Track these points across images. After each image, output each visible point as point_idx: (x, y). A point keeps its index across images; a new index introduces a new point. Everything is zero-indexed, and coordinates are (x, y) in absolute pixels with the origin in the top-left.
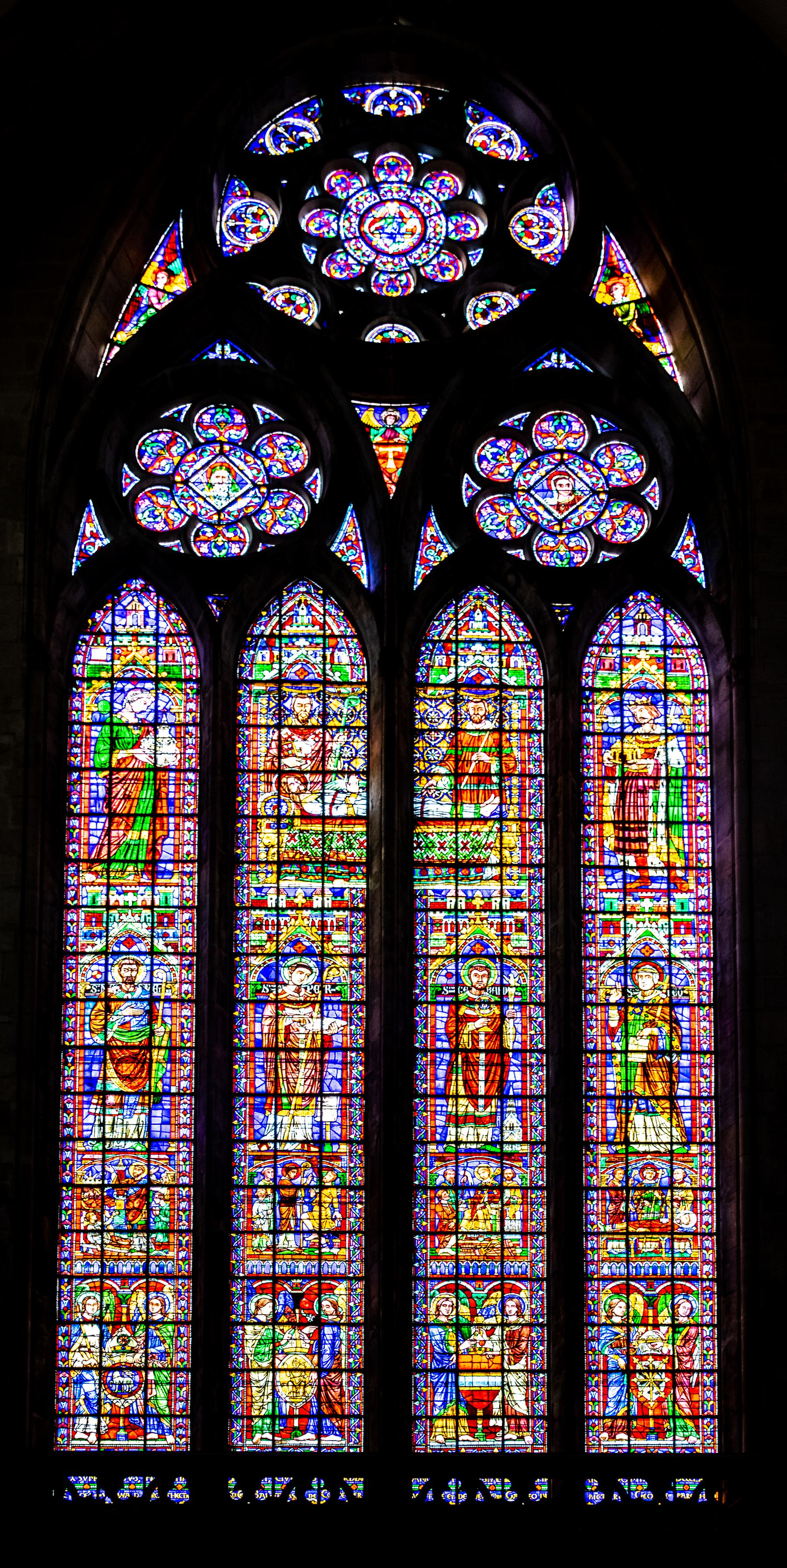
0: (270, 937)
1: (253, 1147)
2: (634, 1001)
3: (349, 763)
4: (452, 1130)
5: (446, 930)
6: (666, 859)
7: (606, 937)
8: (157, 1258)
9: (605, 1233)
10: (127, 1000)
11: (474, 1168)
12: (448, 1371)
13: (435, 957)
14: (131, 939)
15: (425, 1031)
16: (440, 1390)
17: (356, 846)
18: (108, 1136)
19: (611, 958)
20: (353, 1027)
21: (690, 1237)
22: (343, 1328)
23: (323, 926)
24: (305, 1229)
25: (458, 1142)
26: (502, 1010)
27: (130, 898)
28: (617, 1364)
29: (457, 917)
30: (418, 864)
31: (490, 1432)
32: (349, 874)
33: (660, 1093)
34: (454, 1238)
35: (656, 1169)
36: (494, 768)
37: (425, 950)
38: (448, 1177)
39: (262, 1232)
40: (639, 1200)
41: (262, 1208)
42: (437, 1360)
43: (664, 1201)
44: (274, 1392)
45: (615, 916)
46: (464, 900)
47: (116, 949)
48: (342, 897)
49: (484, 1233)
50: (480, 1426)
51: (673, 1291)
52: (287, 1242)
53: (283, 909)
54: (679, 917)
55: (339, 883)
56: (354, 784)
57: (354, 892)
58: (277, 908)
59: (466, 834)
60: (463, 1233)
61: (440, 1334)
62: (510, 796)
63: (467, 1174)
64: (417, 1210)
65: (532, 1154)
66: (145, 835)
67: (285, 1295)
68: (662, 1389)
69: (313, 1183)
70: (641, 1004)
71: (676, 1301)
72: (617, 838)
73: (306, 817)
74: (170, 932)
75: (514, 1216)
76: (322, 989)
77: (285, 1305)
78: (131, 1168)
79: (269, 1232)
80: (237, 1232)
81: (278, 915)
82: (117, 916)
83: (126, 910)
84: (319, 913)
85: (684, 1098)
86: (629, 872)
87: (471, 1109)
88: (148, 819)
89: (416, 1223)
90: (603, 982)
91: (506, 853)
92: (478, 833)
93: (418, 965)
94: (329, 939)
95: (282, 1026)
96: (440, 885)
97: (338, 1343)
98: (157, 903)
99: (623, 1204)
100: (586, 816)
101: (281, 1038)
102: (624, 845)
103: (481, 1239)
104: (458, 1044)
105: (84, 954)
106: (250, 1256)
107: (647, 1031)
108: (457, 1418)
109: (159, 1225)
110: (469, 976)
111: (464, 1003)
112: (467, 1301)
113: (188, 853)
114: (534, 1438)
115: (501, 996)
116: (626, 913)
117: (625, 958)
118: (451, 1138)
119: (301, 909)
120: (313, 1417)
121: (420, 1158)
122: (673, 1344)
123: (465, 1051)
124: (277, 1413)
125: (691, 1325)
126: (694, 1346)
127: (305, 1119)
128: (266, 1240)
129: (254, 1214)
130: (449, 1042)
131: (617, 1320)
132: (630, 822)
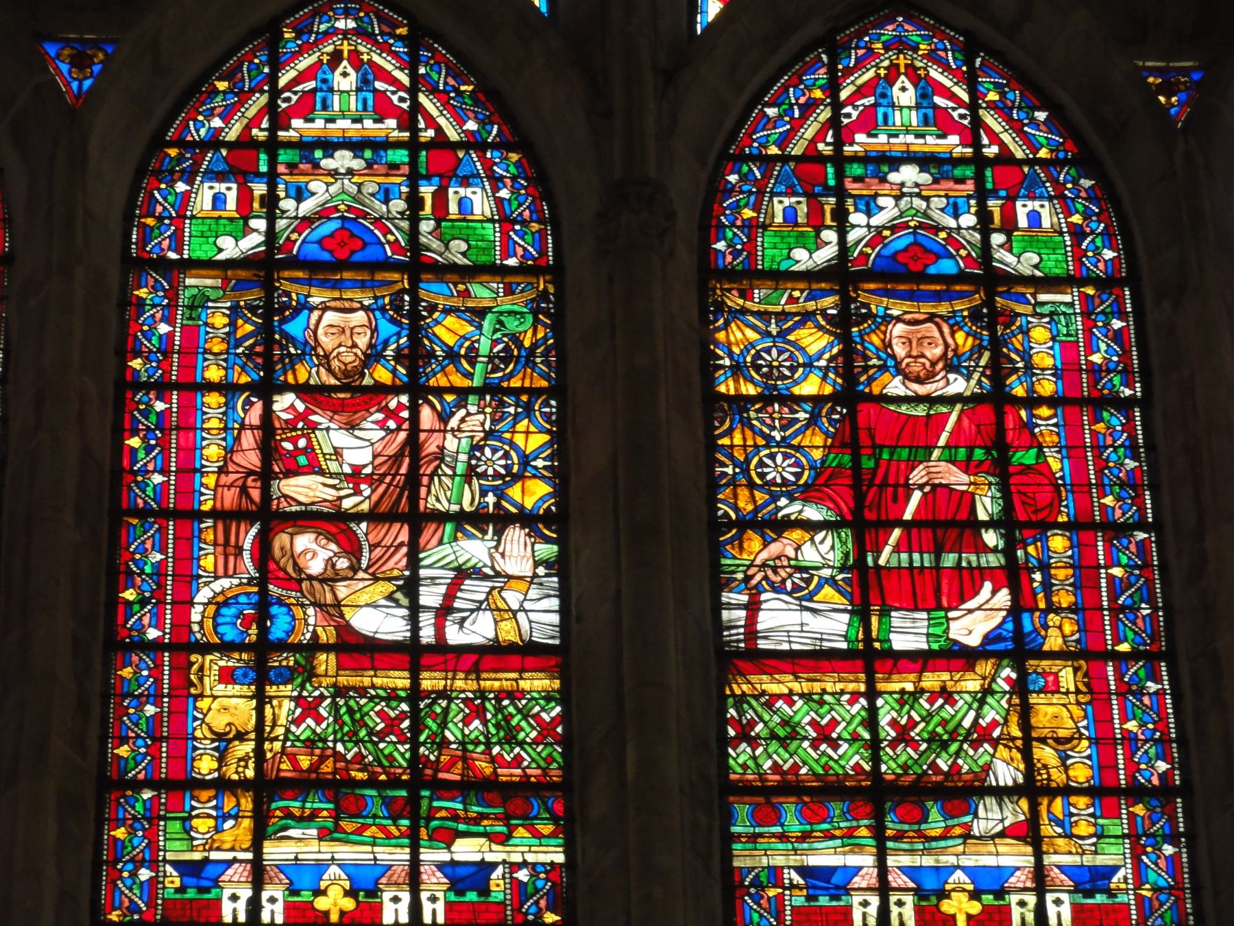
3: (501, 494)
30: (745, 790)
32: (505, 819)
46: (909, 899)
48: (485, 891)
55: (467, 850)
57: (523, 875)
62: (1047, 585)
91: (1046, 754)
92: (947, 695)
96: (824, 857)
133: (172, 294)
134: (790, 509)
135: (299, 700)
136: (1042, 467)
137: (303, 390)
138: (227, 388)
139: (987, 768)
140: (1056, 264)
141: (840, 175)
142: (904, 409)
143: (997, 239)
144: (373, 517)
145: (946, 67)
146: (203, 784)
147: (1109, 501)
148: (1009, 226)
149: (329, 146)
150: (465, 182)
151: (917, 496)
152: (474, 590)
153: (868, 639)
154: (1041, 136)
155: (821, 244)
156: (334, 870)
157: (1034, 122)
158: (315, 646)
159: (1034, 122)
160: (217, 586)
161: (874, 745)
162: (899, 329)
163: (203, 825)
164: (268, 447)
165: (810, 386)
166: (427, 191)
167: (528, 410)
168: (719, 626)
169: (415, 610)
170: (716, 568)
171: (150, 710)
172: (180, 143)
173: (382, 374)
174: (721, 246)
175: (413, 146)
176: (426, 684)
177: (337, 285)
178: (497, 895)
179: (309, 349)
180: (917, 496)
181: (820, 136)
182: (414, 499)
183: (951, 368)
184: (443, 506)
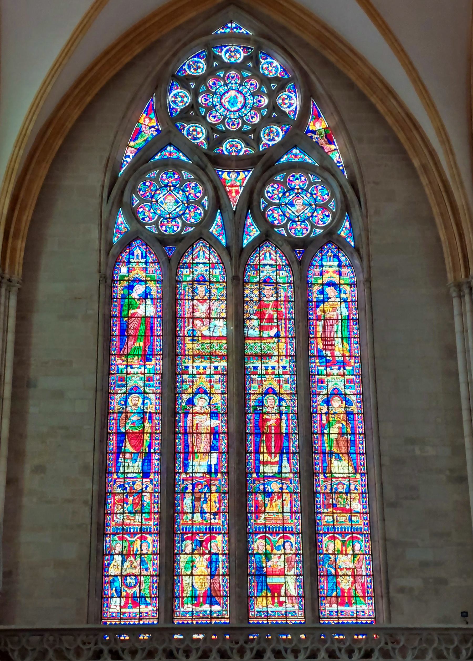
0: (190, 386)
1: (183, 476)
2: (332, 412)
4: (262, 468)
8: (145, 524)
9: (324, 513)
12: (263, 575)
13: (254, 394)
14: (137, 388)
15: (250, 425)
16: (260, 584)
17: (223, 348)
18: (126, 471)
20: (222, 424)
21: (358, 515)
25: (264, 473)
29: (262, 378)
33: (343, 451)
34: (264, 514)
35: (343, 484)
36: (275, 316)
41: (188, 502)
44: (193, 586)
45: (323, 376)
52: (197, 517)
54: (348, 376)
55: (216, 364)
59: (265, 344)
70: (335, 413)
72: (323, 344)
73: (204, 337)
76: (210, 408)
78: (135, 485)
79: (190, 513)
80: (177, 513)
81: (193, 377)
84: (209, 376)
85: (353, 453)
95: (195, 424)
96: (255, 365)
97: (218, 562)
98: (146, 372)
99: (331, 500)
101: (195, 428)
106: (182, 524)
107: (338, 425)
108: (267, 597)
110: (267, 402)
111: (265, 413)
115: (280, 411)
116: (327, 375)
117: (327, 394)
123: (266, 433)
131: (330, 552)
132: (327, 338)
134: (253, 317)
138: (188, 300)
144: (205, 318)
146: (187, 355)
158: (199, 336)
161: (261, 350)
163: (187, 361)
164: (193, 308)
168: (244, 333)
171: (181, 345)
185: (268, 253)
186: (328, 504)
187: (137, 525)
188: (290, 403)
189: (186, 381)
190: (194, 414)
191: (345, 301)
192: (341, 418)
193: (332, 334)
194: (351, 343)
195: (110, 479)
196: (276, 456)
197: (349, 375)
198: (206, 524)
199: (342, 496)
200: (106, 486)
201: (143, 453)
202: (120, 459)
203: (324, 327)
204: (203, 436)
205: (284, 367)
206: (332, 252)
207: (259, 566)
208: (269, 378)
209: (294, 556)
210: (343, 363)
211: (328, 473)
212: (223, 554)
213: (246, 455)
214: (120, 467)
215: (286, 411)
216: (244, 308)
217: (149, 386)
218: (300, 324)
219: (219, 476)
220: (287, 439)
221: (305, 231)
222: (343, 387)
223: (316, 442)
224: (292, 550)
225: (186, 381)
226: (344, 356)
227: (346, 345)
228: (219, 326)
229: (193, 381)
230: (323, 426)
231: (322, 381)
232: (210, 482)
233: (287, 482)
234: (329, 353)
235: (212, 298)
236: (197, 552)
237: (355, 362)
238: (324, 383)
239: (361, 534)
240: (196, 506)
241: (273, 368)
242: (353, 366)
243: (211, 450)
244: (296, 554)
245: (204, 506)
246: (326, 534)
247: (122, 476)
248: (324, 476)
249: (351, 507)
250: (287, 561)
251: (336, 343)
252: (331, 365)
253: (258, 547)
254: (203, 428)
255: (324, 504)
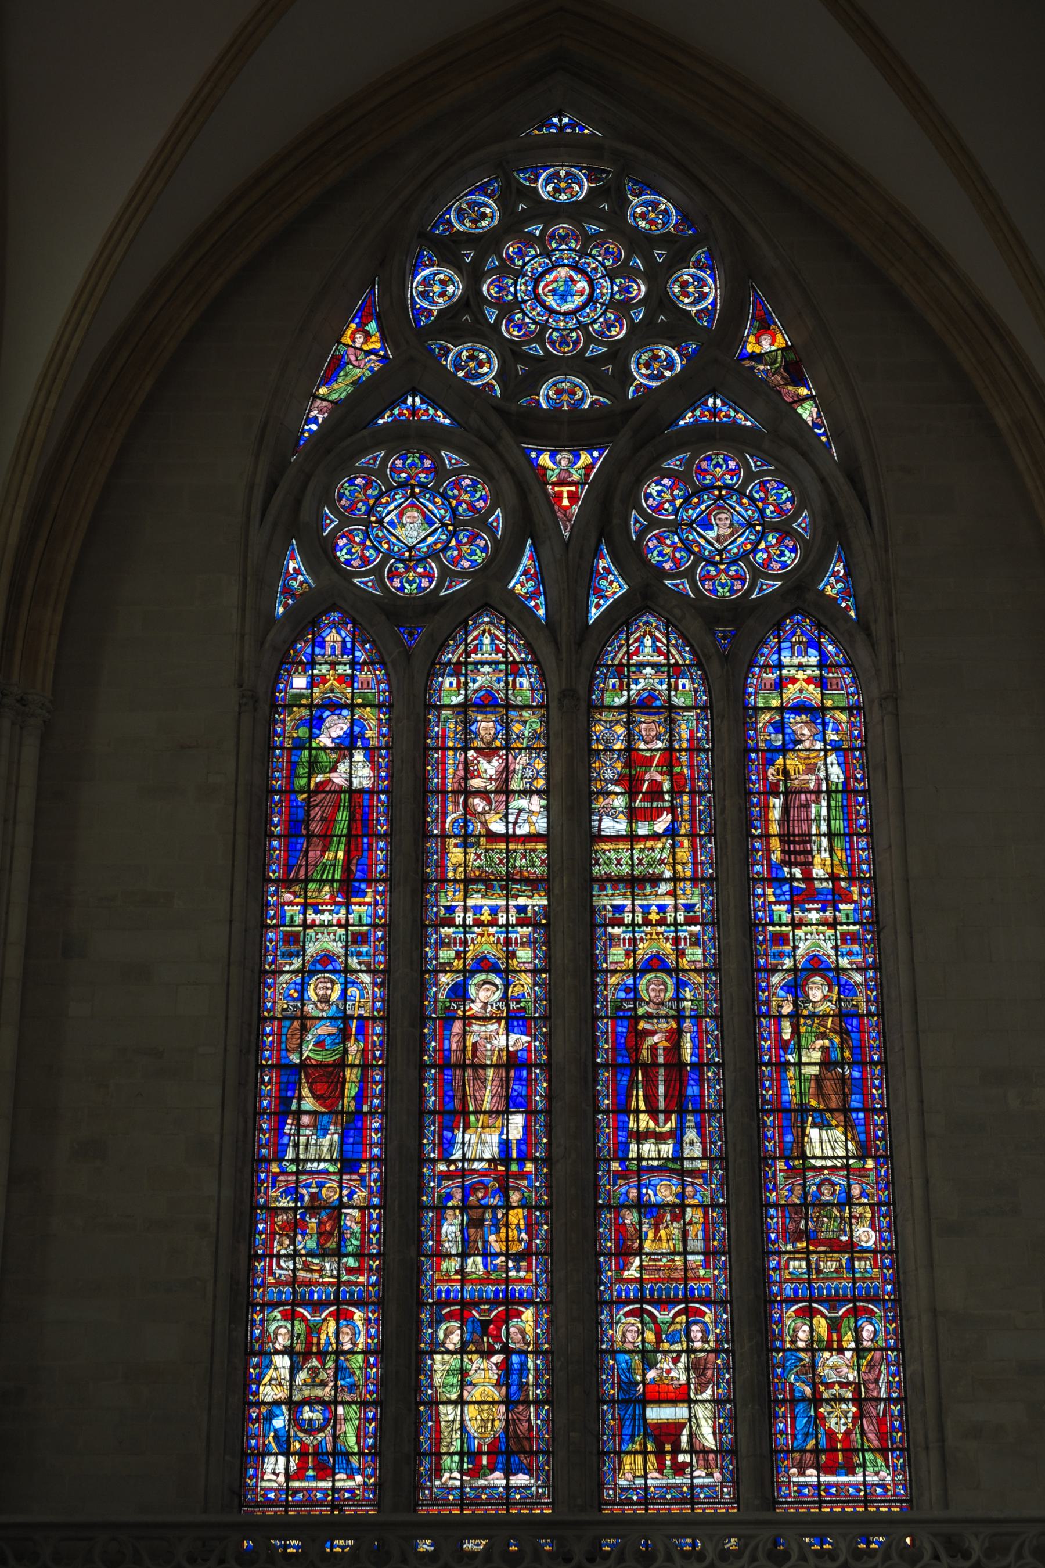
0: (458, 953)
1: (442, 1167)
2: (805, 1012)
3: (531, 784)
4: (634, 1147)
5: (624, 945)
6: (829, 870)
7: (776, 949)
8: (349, 1283)
9: (786, 1252)
10: (322, 1018)
11: (655, 1186)
12: (637, 1401)
13: (615, 971)
14: (327, 958)
15: (606, 1047)
16: (627, 1423)
17: (538, 863)
18: (301, 1156)
19: (782, 970)
20: (537, 1043)
21: (869, 1255)
22: (531, 1356)
23: (508, 942)
24: (493, 1251)
25: (640, 1158)
26: (679, 1024)
27: (326, 917)
28: (803, 1393)
29: (634, 932)
30: (597, 880)
31: (679, 1469)
32: (531, 891)
33: (833, 1105)
34: (638, 1259)
35: (833, 1184)
36: (666, 787)
37: (605, 965)
38: (631, 1195)
39: (449, 1256)
40: (818, 1218)
41: (450, 1229)
42: (624, 1390)
43: (842, 1218)
44: (463, 1428)
45: (784, 928)
46: (640, 915)
47: (313, 968)
49: (667, 1254)
50: (668, 1463)
51: (855, 1312)
52: (475, 1265)
53: (470, 926)
54: (845, 927)
55: (522, 901)
56: (536, 803)
57: (536, 908)
58: (464, 925)
59: (641, 851)
60: (647, 1254)
61: (626, 1362)
62: (682, 812)
63: (650, 1192)
64: (601, 1230)
65: (711, 1170)
66: (341, 855)
67: (473, 1321)
68: (850, 1420)
69: (500, 1203)
70: (813, 1015)
71: (859, 1323)
72: (783, 851)
73: (492, 837)
74: (364, 949)
75: (696, 1235)
76: (508, 1006)
77: (473, 1332)
78: (324, 1191)
79: (457, 1255)
80: (426, 1256)
81: (465, 933)
82: (313, 934)
83: (322, 929)
84: (503, 929)
85: (857, 1110)
86: (795, 884)
87: (652, 1125)
88: (344, 839)
89: (600, 1244)
90: (775, 994)
91: (679, 868)
92: (653, 849)
93: (598, 980)
94: (512, 955)
96: (618, 902)
98: (351, 921)
99: (803, 1222)
100: (753, 831)
101: (469, 1054)
102: (790, 858)
103: (665, 1260)
104: (637, 1059)
105: (283, 972)
106: (439, 1281)
107: (819, 1043)
108: (644, 1453)
109: (350, 1249)
110: (647, 990)
111: (642, 1017)
112: (652, 1326)
113: (381, 873)
114: (723, 1475)
115: (678, 1010)
116: (796, 924)
117: (794, 970)
118: (633, 1154)
119: (488, 925)
120: (502, 1453)
121: (603, 1176)
122: (859, 1370)
123: (645, 1066)
124: (466, 1450)
125: (875, 1350)
126: (880, 1372)
127: (493, 1138)
128: (454, 1264)
129: (443, 1236)
130: (629, 1057)
131: (801, 1344)
132: (794, 835)
133: (439, 717)
134: (612, 788)
135: (476, 854)
136: (682, 773)
137: (476, 749)
138: (455, 749)
139: (663, 872)
140: (689, 702)
141: (629, 671)
142: (644, 753)
143: (673, 693)
144: (496, 792)
145: (661, 632)
146: (450, 881)
147: (700, 783)
148: (676, 689)
149: (483, 663)
150: (521, 676)
151: (647, 783)
152: (524, 816)
153: (632, 831)
154: (687, 656)
155: (622, 696)
156: (485, 908)
157: (685, 651)
158: (480, 835)
159: (685, 651)
160: (454, 815)
161: (632, 866)
162: (644, 725)
163: (450, 894)
164: (466, 769)
165: (618, 746)
166: (510, 679)
167: (539, 756)
168: (591, 827)
169: (507, 823)
170: (590, 808)
171: (435, 857)
172: (440, 663)
173: (498, 743)
174: (594, 697)
175: (506, 663)
176: (510, 847)
177: (485, 713)
178: (530, 914)
179: (477, 734)
180: (647, 783)
181: (623, 657)
182: (507, 786)
183: (659, 739)
184: (515, 788)
185: (648, 637)
186: (794, 1232)
187: (329, 1283)
188: (703, 992)
189: (449, 944)
190: (468, 1020)
191: (836, 748)
192: (829, 1026)
193: (805, 827)
194: (852, 849)
195: (263, 1175)
196: (667, 1120)
197: (848, 924)
198: (497, 1282)
199: (831, 1211)
200: (254, 1189)
201: (342, 1112)
202: (288, 1127)
203: (786, 810)
204: (490, 1072)
205: (689, 907)
206: (803, 633)
207: (626, 1380)
208: (651, 934)
209: (712, 1356)
210: (833, 895)
211: (798, 1158)
212: (537, 1353)
213: (594, 1117)
214: (287, 1145)
215: (692, 1010)
216: (590, 767)
217: (359, 954)
218: (727, 802)
219: (529, 1167)
220: (695, 1077)
221: (738, 586)
222: (832, 952)
223: (767, 1084)
224: (708, 1342)
225: (449, 944)
226: (834, 878)
227: (839, 853)
228: (531, 812)
229: (464, 943)
230: (783, 1046)
231: (781, 939)
232: (508, 1182)
233: (696, 1181)
234: (797, 872)
235: (514, 745)
236: (474, 1349)
237: (861, 893)
238: (788, 945)
239: (876, 1300)
240: (472, 1238)
241: (662, 908)
242: (855, 902)
243: (508, 1106)
244: (716, 1351)
245: (492, 1238)
246: (790, 1301)
247: (293, 1168)
248: (787, 1164)
249: (851, 1237)
250: (696, 1369)
251: (815, 848)
252: (804, 902)
253: (624, 1335)
254: (489, 1053)
255: (785, 1230)
